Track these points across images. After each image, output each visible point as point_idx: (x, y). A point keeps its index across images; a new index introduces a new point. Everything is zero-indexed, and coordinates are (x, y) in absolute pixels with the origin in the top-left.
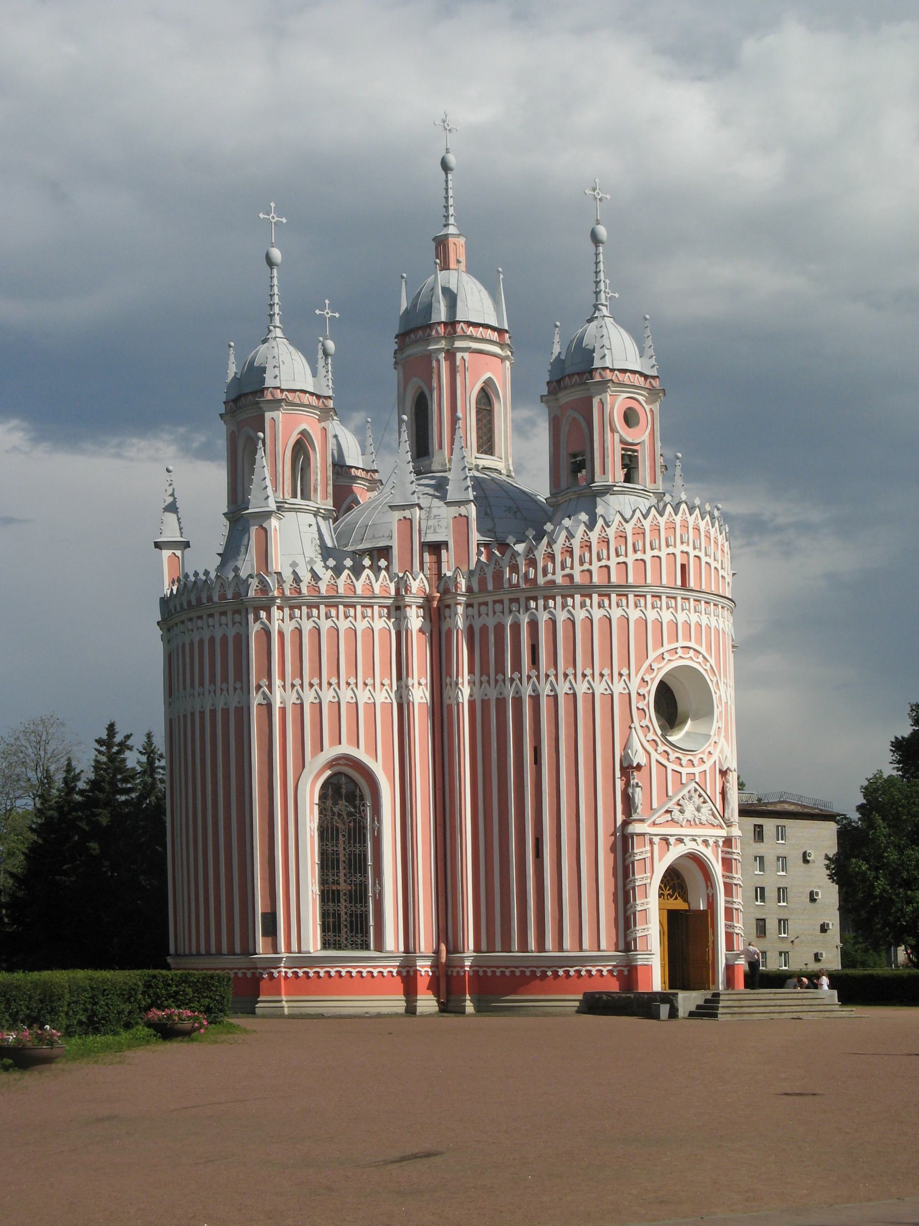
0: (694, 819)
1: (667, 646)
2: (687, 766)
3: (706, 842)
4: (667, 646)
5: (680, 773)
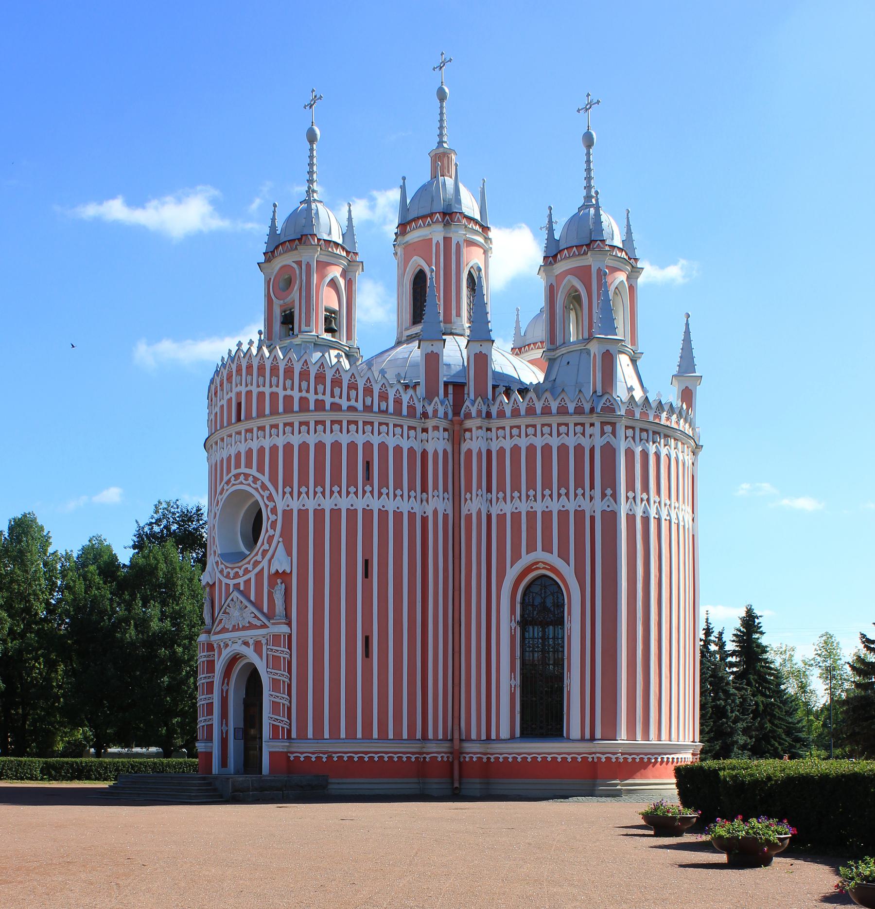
0: (238, 624)
1: (225, 479)
2: (234, 578)
3: (246, 644)
4: (225, 479)
5: (229, 585)
